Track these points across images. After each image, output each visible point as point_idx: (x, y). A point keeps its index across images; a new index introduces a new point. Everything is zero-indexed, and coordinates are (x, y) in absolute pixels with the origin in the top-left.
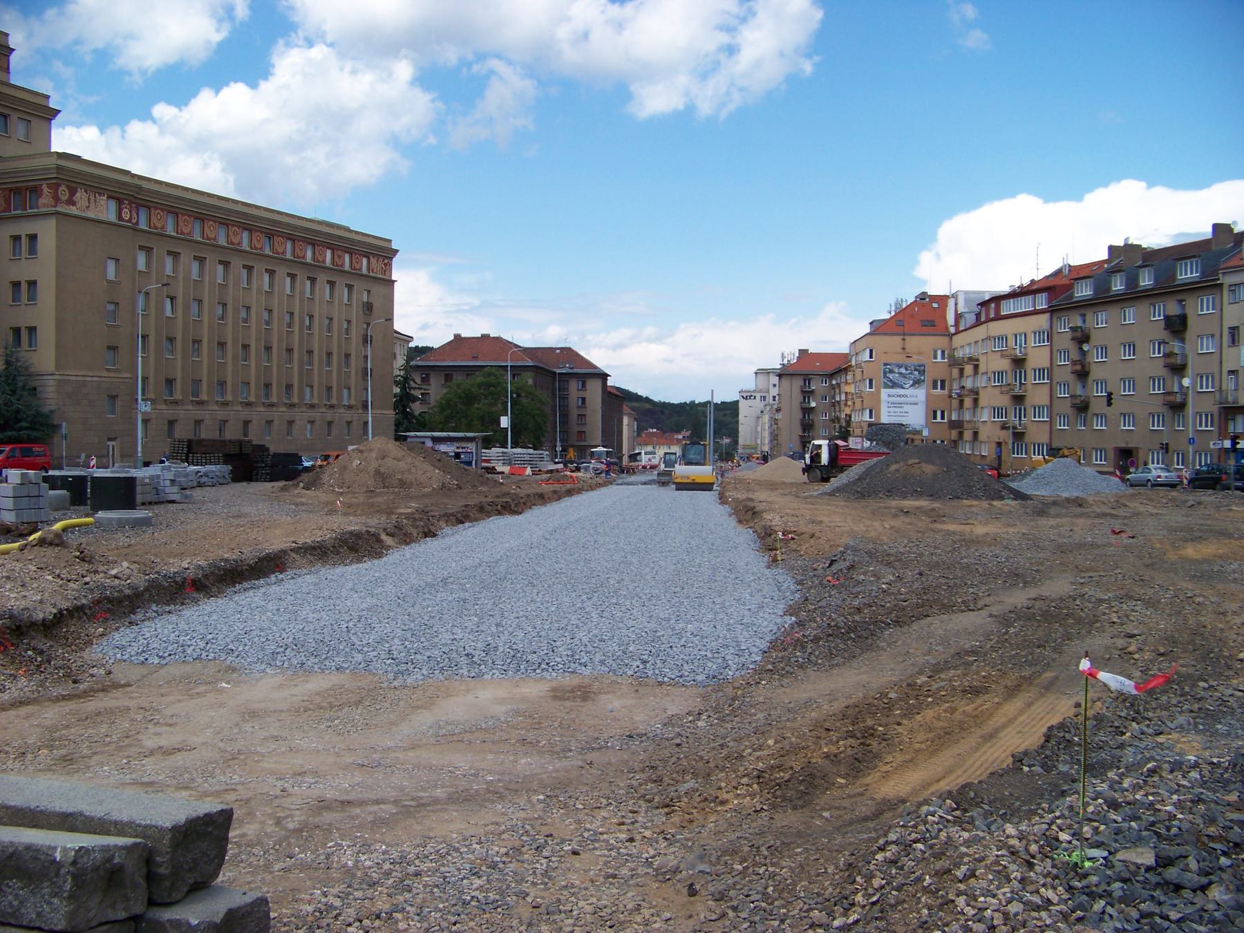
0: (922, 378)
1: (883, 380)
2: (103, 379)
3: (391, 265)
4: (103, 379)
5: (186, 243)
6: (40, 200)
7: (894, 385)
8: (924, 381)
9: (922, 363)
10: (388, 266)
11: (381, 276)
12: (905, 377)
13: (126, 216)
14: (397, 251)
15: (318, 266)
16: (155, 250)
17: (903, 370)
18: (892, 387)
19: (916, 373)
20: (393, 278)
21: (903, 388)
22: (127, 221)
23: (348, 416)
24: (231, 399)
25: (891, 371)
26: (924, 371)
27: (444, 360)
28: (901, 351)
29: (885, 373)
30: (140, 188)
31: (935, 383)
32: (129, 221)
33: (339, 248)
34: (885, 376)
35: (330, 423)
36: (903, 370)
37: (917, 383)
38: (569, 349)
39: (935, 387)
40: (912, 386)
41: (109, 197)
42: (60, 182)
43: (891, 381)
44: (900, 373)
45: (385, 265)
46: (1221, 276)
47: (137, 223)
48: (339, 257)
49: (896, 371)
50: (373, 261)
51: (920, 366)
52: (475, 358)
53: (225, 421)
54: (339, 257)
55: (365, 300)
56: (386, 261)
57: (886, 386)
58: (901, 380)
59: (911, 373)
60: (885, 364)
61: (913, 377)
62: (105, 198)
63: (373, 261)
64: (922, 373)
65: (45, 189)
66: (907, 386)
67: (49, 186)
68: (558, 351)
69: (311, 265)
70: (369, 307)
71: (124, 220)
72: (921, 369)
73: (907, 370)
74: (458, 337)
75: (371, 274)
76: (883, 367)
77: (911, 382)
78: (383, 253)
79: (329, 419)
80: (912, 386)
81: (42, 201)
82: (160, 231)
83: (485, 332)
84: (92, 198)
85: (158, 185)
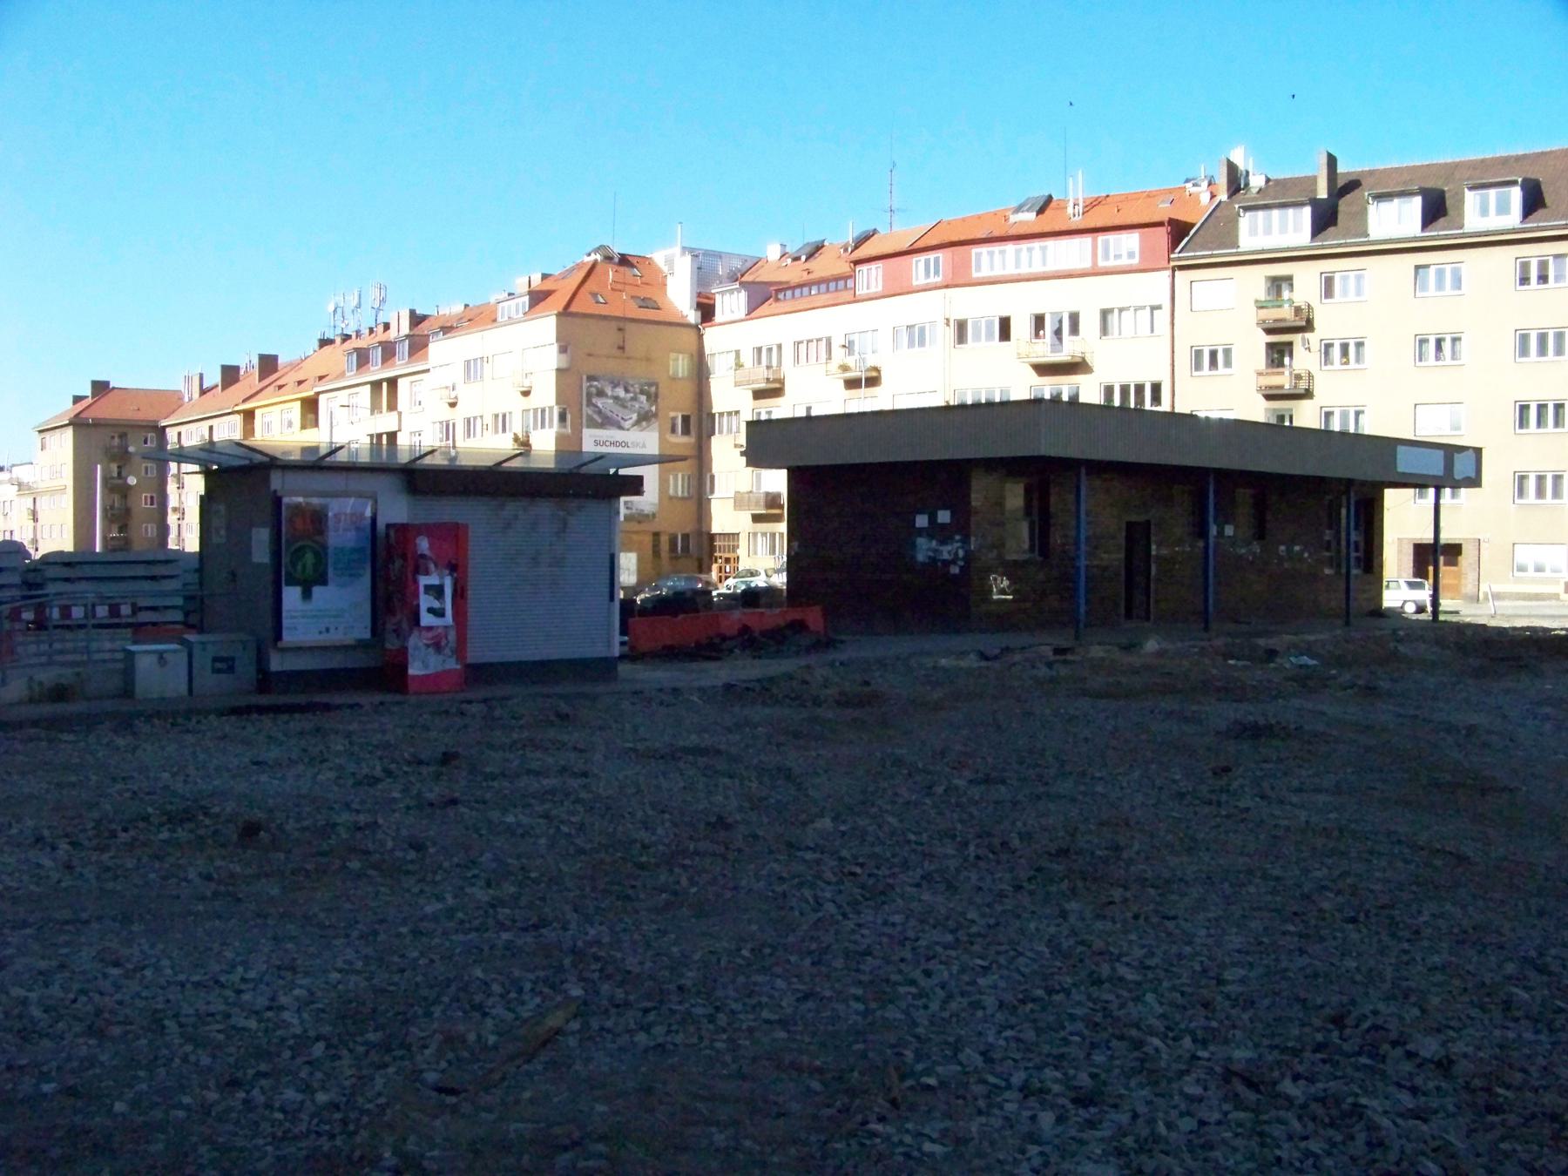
0: (653, 408)
1: (587, 411)
8: (655, 415)
12: (625, 407)
17: (621, 392)
18: (602, 426)
19: (643, 398)
21: (621, 428)
25: (601, 394)
26: (656, 396)
28: (619, 353)
29: (589, 396)
34: (590, 403)
36: (621, 392)
37: (644, 418)
40: (638, 423)
43: (600, 412)
44: (616, 398)
49: (610, 393)
51: (650, 385)
57: (593, 424)
59: (634, 399)
60: (591, 378)
64: (653, 398)
66: (627, 424)
73: (627, 391)
76: (585, 385)
77: (635, 416)
80: (638, 423)
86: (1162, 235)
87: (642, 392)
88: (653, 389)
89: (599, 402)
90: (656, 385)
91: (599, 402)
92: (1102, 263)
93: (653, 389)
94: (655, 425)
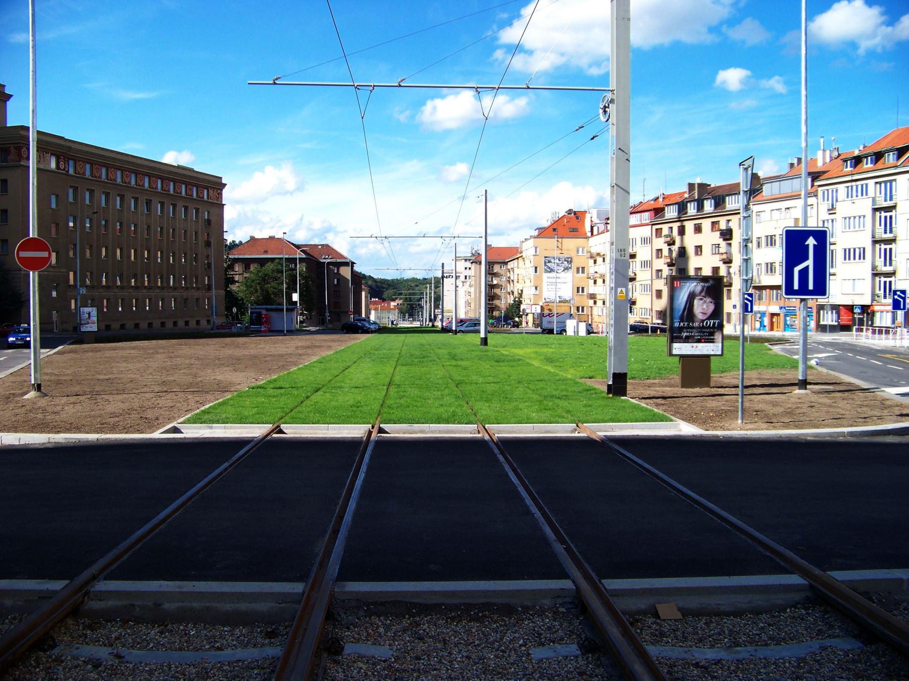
2: (50, 273)
3: (221, 194)
4: (50, 273)
5: (98, 183)
6: (9, 157)
7: (552, 271)
8: (571, 268)
9: (569, 256)
10: (220, 194)
11: (216, 202)
13: (62, 167)
14: (226, 184)
15: (177, 196)
16: (79, 188)
18: (550, 272)
19: (566, 262)
20: (223, 203)
22: (63, 170)
23: (196, 294)
24: (140, 285)
25: (549, 262)
26: (571, 262)
27: (244, 254)
29: (545, 263)
30: (70, 148)
31: (578, 269)
32: (64, 170)
33: (190, 184)
34: (545, 265)
35: (186, 299)
37: (566, 269)
38: (327, 246)
39: (578, 272)
41: (52, 154)
42: (22, 145)
45: (218, 194)
46: (751, 206)
47: (68, 171)
48: (190, 189)
49: (553, 261)
50: (211, 191)
51: (568, 258)
52: (266, 252)
53: (198, 299)
54: (190, 189)
55: (206, 218)
56: (219, 191)
57: (546, 271)
58: (556, 268)
59: (562, 263)
60: (545, 257)
61: (563, 265)
62: (49, 155)
63: (211, 191)
65: (13, 150)
67: (15, 148)
68: (320, 247)
69: (185, 197)
70: (209, 222)
71: (61, 170)
72: (570, 261)
73: (559, 260)
74: (252, 238)
75: (210, 200)
76: (544, 259)
77: (563, 269)
78: (216, 185)
79: (185, 297)
81: (9, 157)
82: (82, 176)
83: (272, 235)
84: (42, 155)
85: (80, 145)
86: (653, 213)
87: (565, 261)
88: (570, 259)
89: (549, 265)
90: (571, 258)
91: (549, 265)
92: (643, 222)
93: (570, 259)
94: (570, 271)
